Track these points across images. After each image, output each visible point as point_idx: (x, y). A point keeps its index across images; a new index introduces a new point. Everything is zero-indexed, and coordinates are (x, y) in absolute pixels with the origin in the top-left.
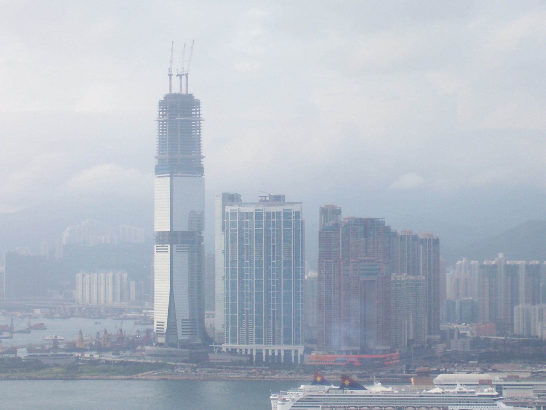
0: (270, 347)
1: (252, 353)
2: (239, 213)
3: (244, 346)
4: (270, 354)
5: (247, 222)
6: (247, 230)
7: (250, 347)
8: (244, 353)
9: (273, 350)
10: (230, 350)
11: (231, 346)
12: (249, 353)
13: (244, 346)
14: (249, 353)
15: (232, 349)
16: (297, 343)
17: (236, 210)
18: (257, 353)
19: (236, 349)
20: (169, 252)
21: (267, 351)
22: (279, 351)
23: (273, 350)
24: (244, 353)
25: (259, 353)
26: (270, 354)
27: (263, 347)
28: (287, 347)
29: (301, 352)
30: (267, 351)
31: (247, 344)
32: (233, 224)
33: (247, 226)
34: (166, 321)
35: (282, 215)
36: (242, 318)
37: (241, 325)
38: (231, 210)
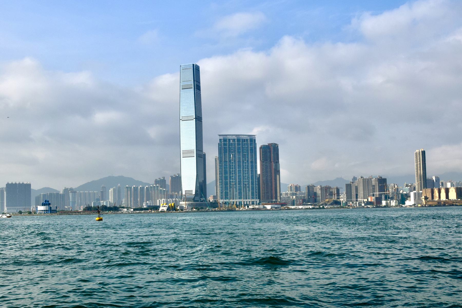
0: (245, 200)
4: (245, 203)
7: (235, 200)
9: (247, 202)
16: (256, 198)
20: (195, 157)
21: (244, 202)
22: (249, 202)
23: (247, 202)
25: (240, 203)
26: (245, 203)
27: (242, 200)
28: (253, 200)
29: (258, 202)
30: (244, 202)
32: (225, 145)
33: (232, 145)
35: (249, 141)
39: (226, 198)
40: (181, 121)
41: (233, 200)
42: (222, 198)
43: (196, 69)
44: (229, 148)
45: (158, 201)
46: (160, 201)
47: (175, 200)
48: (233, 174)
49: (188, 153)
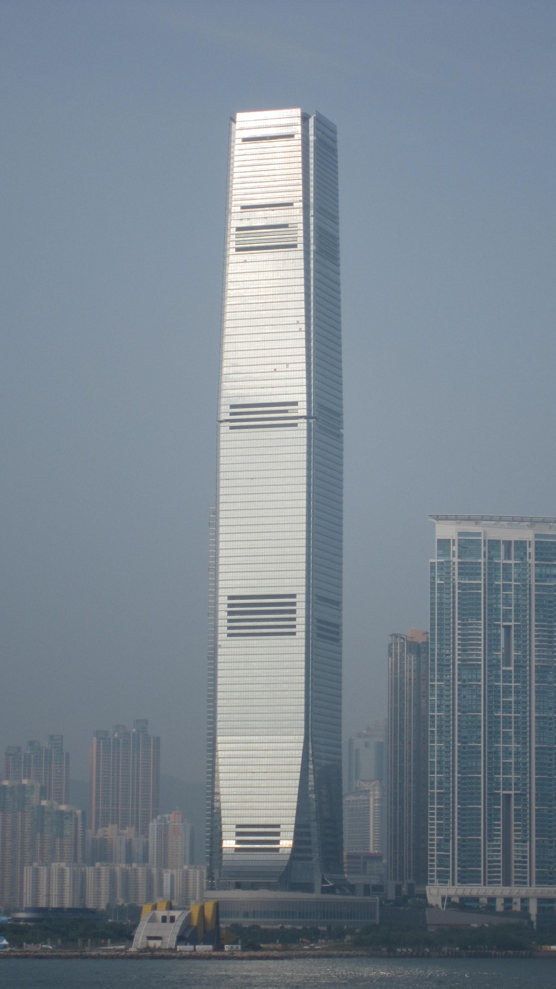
1: (525, 909)
2: (485, 541)
3: (499, 891)
5: (507, 567)
6: (507, 587)
8: (499, 906)
10: (456, 900)
11: (456, 890)
12: (517, 908)
13: (499, 891)
14: (517, 908)
15: (463, 899)
17: (479, 534)
18: (539, 909)
19: (476, 899)
24: (499, 906)
31: (507, 883)
33: (507, 577)
34: (287, 820)
36: (492, 815)
37: (490, 837)
38: (460, 534)
39: (466, 878)
40: (224, 428)
41: (506, 891)
42: (443, 877)
43: (318, 141)
44: (492, 589)
45: (28, 871)
46: (36, 873)
47: (126, 875)
48: (507, 739)
49: (259, 614)
